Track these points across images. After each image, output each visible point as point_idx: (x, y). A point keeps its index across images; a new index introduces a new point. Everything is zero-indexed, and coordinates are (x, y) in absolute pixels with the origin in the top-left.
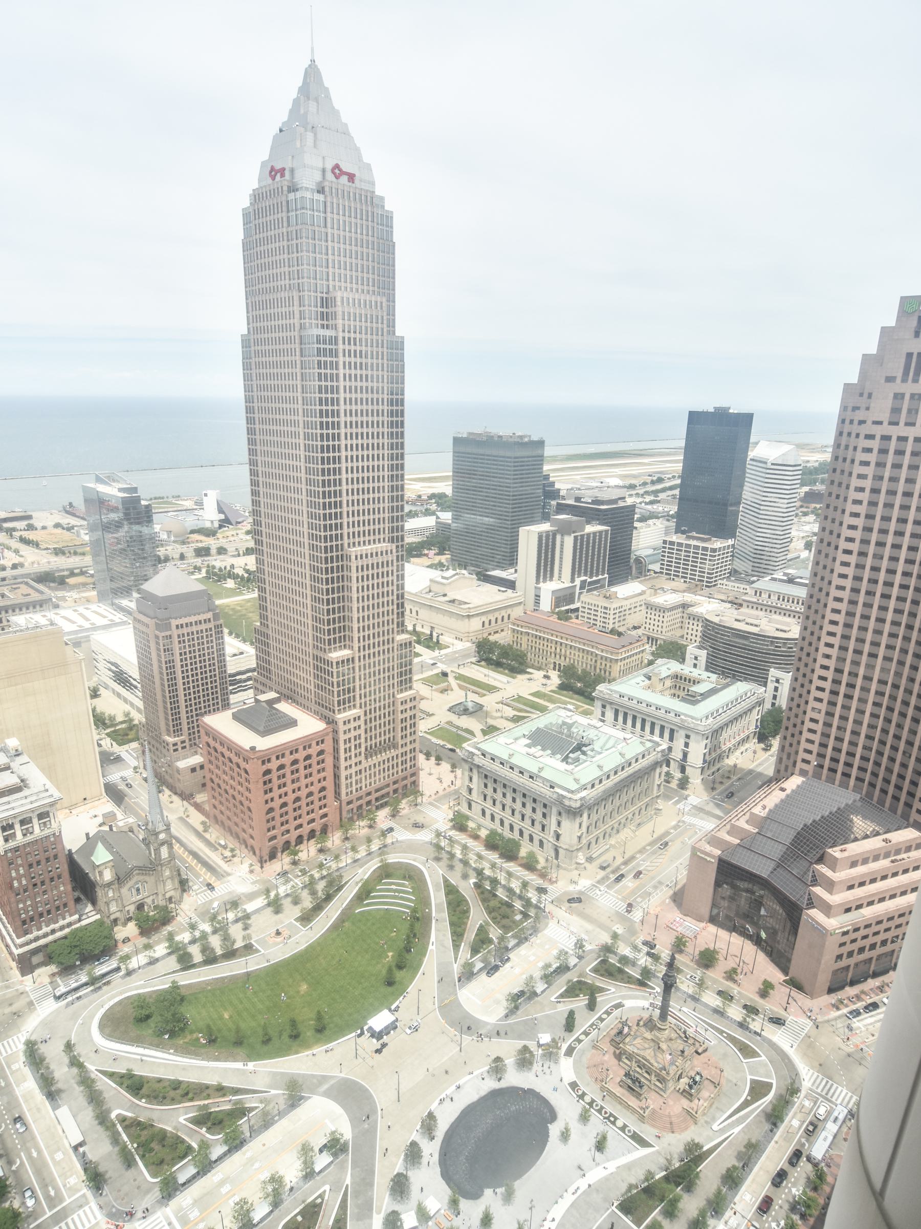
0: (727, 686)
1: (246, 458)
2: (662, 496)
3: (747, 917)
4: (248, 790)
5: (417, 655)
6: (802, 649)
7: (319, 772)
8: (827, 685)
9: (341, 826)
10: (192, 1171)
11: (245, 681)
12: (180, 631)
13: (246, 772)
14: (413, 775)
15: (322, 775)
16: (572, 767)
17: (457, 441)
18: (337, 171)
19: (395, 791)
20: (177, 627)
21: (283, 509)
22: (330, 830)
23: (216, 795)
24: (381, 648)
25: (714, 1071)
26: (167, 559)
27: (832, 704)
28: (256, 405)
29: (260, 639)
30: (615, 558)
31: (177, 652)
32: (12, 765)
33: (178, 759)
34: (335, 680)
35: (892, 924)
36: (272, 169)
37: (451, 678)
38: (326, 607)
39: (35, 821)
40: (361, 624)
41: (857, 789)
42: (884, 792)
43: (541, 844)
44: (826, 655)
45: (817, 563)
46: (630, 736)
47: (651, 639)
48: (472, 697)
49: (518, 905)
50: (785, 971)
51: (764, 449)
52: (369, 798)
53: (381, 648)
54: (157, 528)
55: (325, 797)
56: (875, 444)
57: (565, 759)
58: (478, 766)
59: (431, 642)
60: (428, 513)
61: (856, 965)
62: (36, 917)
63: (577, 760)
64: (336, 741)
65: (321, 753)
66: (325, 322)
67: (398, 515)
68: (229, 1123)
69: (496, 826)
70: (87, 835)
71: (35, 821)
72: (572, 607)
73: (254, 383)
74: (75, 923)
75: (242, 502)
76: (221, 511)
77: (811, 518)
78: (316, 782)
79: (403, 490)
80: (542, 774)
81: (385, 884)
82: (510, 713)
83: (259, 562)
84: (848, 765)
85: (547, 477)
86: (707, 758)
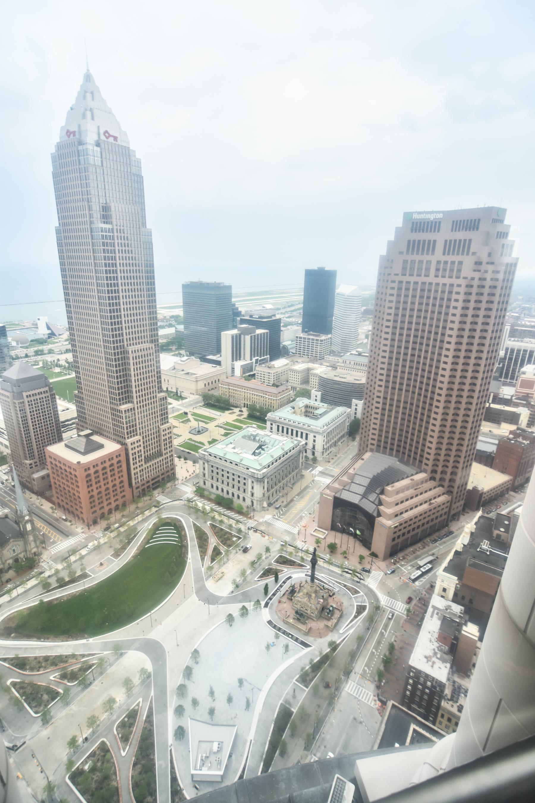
0: (333, 409)
1: (62, 297)
2: (295, 313)
3: (350, 525)
4: (78, 487)
5: (170, 404)
6: (367, 388)
8: (380, 406)
11: (71, 425)
12: (29, 399)
13: (76, 476)
15: (121, 474)
17: (185, 286)
18: (107, 135)
19: (163, 479)
20: (27, 396)
21: (88, 326)
22: (127, 503)
23: (58, 491)
24: (150, 401)
26: (17, 358)
27: (383, 415)
28: (66, 267)
29: (79, 401)
30: (272, 347)
31: (28, 411)
33: (33, 473)
34: (124, 421)
35: (417, 520)
36: (68, 131)
37: (190, 416)
38: (116, 380)
40: (137, 389)
41: (396, 456)
42: (409, 456)
43: (244, 499)
44: (379, 391)
45: (372, 345)
47: (294, 388)
48: (202, 424)
49: (234, 533)
50: (369, 548)
51: (343, 288)
52: (148, 484)
53: (150, 401)
54: (9, 339)
55: (123, 486)
56: (396, 285)
57: (254, 454)
58: (208, 461)
59: (178, 396)
60: (170, 326)
63: (260, 453)
65: (119, 462)
66: (105, 220)
67: (154, 328)
68: (79, 674)
69: (219, 492)
72: (252, 373)
73: (65, 254)
75: (61, 323)
76: (49, 328)
77: (367, 323)
78: (117, 478)
79: (156, 313)
82: (223, 431)
83: (74, 356)
84: (392, 444)
85: (234, 305)
86: (325, 447)
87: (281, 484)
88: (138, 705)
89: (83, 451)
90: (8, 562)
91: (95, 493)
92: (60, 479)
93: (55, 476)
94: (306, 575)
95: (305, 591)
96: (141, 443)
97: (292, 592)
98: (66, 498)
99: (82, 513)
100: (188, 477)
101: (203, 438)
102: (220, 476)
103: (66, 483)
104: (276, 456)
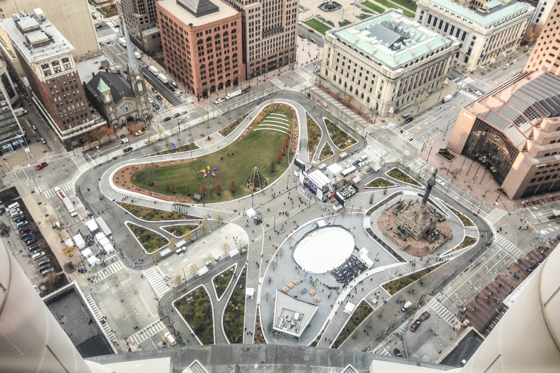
7: (233, 43)
9: (247, 79)
10: (168, 251)
13: (187, 40)
14: (292, 50)
15: (235, 46)
16: (395, 52)
22: (239, 81)
23: (169, 54)
25: (446, 230)
32: (41, 26)
33: (143, 29)
39: (61, 63)
43: (368, 100)
46: (437, 34)
52: (264, 63)
55: (236, 60)
57: (392, 47)
61: (543, 185)
62: (71, 120)
63: (399, 48)
64: (244, 24)
65: (234, 31)
69: (342, 86)
70: (93, 74)
71: (61, 63)
74: (93, 125)
80: (374, 55)
81: (272, 116)
87: (416, 91)
88: (234, 268)
89: (195, 11)
90: (122, 118)
91: (207, 63)
92: (171, 40)
93: (166, 37)
94: (419, 195)
95: (413, 210)
96: (261, 12)
97: (400, 206)
98: (177, 63)
99: (192, 82)
100: (309, 63)
101: (333, 17)
102: (345, 68)
103: (177, 46)
104: (418, 55)
